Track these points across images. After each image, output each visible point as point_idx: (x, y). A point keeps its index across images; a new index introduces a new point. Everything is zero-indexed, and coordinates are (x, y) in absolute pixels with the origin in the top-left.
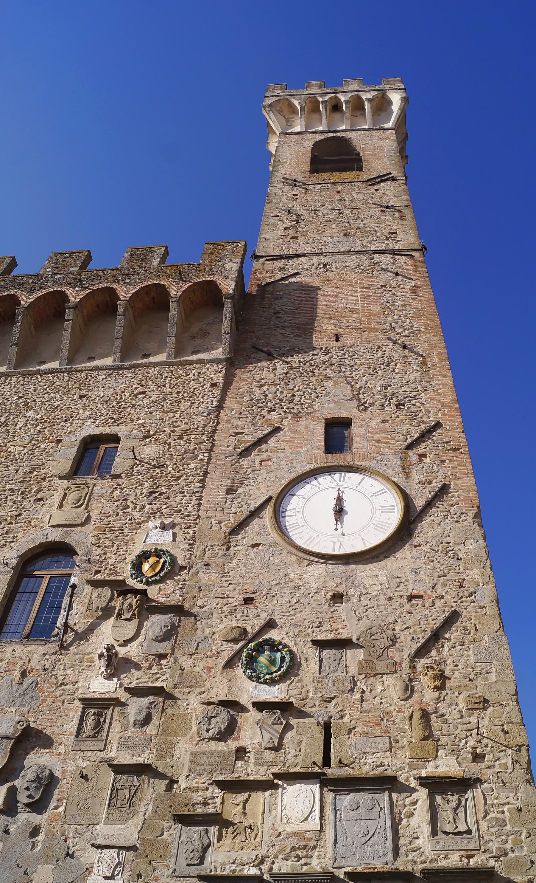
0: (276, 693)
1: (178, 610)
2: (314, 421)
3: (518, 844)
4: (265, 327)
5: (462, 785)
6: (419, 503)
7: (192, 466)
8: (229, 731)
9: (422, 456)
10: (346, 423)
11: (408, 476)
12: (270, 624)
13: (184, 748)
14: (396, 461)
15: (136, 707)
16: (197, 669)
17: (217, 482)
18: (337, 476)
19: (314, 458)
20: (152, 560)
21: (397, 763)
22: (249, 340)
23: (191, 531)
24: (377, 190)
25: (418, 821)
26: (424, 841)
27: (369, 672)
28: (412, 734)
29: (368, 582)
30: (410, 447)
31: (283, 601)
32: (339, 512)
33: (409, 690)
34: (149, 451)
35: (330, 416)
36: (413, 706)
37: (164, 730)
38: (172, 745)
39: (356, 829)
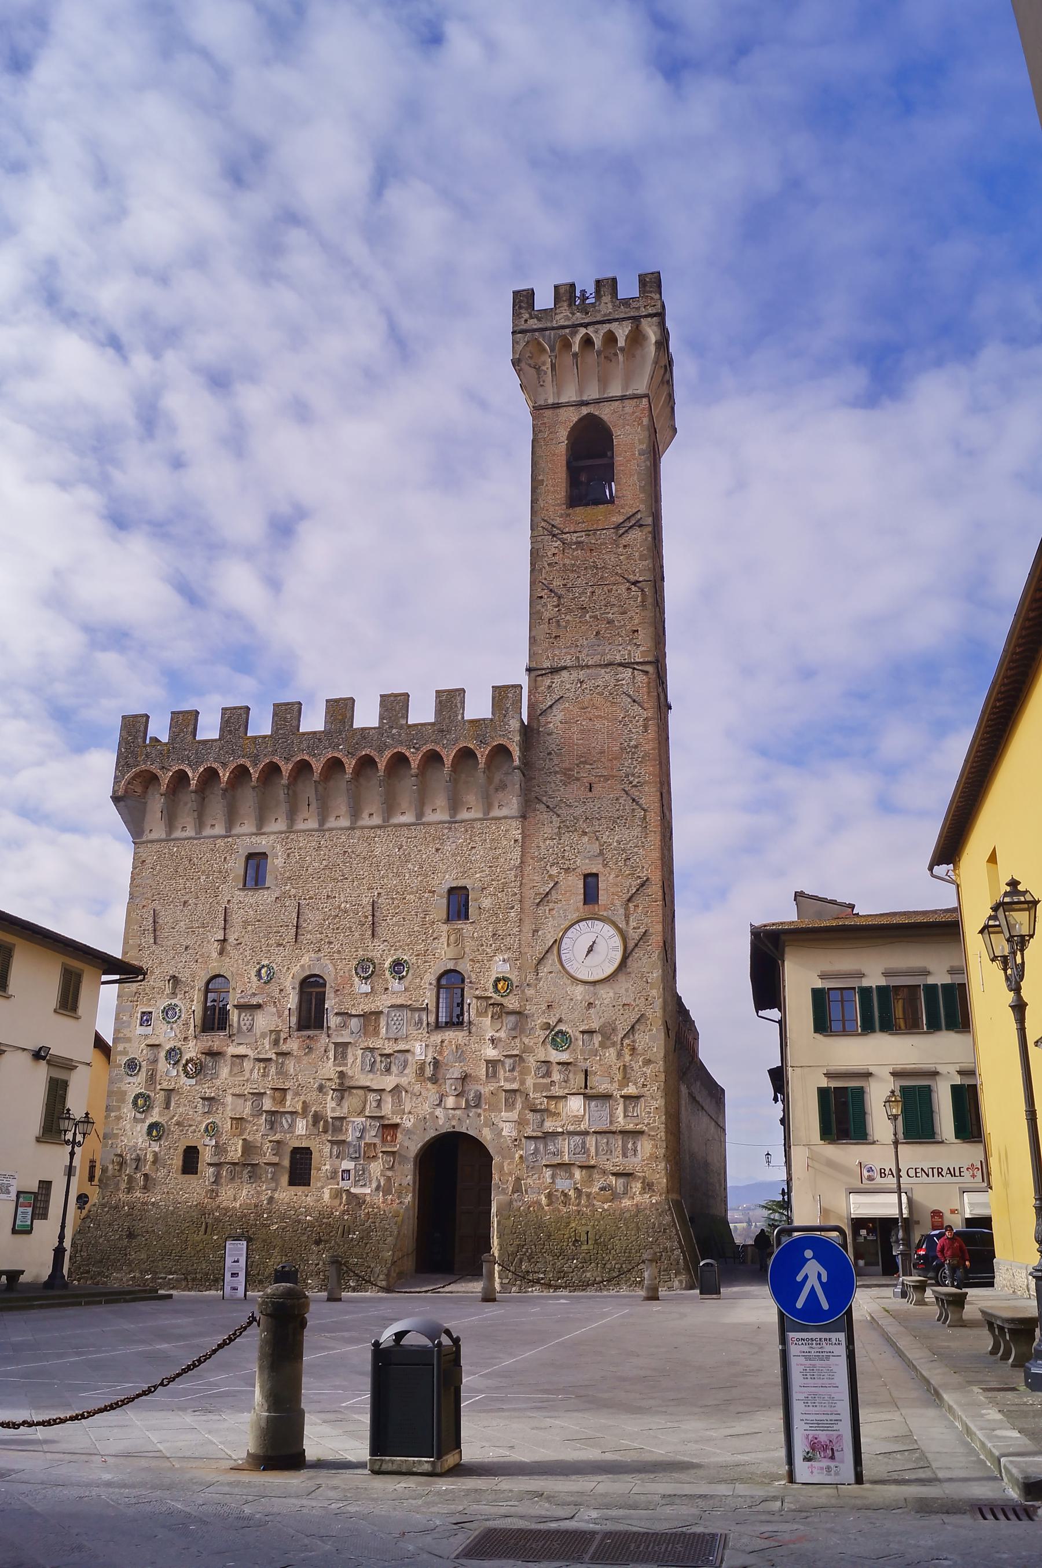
0: (564, 1057)
1: (519, 1013)
3: (654, 1121)
5: (637, 1098)
6: (631, 944)
8: (548, 1074)
9: (637, 906)
10: (596, 875)
11: (627, 923)
12: (560, 1021)
13: (530, 1082)
14: (622, 911)
15: (509, 1062)
17: (528, 928)
18: (590, 922)
19: (578, 909)
20: (502, 983)
21: (612, 1088)
23: (518, 962)
24: (625, 546)
25: (620, 1111)
26: (621, 1119)
27: (602, 1045)
28: (619, 1076)
29: (604, 996)
30: (629, 900)
31: (565, 1007)
32: (590, 950)
33: (619, 1055)
35: (586, 872)
36: (620, 1064)
37: (521, 1073)
39: (596, 1114)
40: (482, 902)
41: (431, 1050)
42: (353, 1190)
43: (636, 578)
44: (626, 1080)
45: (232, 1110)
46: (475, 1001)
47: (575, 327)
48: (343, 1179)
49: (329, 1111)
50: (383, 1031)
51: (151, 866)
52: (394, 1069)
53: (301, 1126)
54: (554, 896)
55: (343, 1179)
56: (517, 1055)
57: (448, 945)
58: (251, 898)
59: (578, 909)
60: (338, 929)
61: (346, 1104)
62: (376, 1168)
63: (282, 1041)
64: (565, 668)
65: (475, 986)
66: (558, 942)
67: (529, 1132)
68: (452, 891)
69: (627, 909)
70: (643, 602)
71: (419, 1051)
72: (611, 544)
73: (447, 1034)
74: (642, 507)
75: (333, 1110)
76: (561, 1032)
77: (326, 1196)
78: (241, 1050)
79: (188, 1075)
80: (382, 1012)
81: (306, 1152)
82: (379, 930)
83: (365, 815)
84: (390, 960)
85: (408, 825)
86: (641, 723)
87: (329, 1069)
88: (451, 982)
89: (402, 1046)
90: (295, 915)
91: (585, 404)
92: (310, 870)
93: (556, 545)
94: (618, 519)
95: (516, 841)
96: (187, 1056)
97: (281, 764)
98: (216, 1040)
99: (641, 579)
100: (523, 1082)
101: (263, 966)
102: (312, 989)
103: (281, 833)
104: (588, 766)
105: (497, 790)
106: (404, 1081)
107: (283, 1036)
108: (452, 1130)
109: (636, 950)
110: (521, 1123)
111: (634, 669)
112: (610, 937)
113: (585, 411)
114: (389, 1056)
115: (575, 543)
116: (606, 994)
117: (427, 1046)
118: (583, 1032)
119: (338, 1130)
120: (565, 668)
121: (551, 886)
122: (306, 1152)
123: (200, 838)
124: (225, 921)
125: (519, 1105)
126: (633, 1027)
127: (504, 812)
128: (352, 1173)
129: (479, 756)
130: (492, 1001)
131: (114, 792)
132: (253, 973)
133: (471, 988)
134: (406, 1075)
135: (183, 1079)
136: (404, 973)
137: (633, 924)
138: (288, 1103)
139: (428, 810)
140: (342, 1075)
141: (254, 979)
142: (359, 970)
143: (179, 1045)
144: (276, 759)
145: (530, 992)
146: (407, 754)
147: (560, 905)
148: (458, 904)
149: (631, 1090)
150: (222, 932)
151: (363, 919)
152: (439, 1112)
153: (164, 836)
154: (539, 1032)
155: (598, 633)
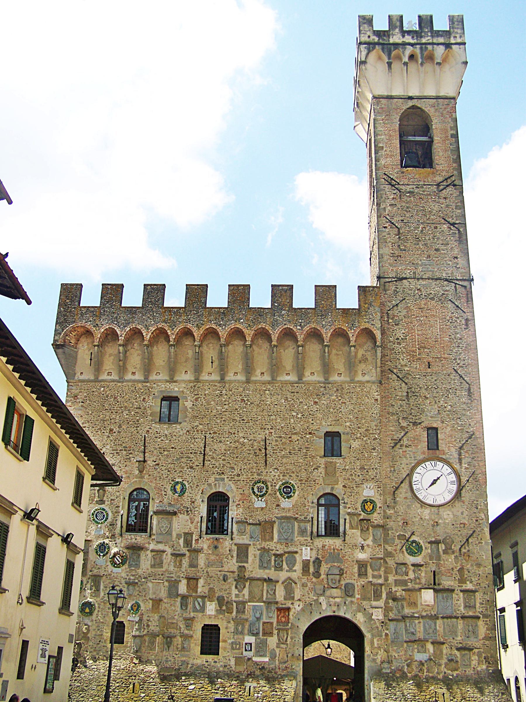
2: (422, 428)
4: (393, 352)
7: (374, 454)
14: (456, 456)
16: (391, 550)
19: (424, 453)
22: (387, 363)
24: (445, 198)
26: (462, 608)
32: (434, 482)
34: (355, 444)
37: (385, 572)
38: (388, 577)
40: (351, 445)
41: (314, 552)
42: (254, 659)
43: (453, 221)
44: (462, 581)
45: (154, 593)
46: (347, 517)
47: (404, 44)
48: (246, 650)
49: (233, 596)
50: (276, 536)
51: (81, 400)
52: (285, 566)
53: (211, 608)
54: (405, 442)
55: (246, 650)
56: (381, 559)
57: (326, 473)
58: (165, 430)
59: (424, 453)
60: (237, 457)
61: (246, 591)
62: (272, 641)
63: (194, 542)
64: (406, 278)
65: (348, 506)
66: (410, 475)
67: (391, 615)
68: (327, 434)
69: (460, 454)
70: (460, 238)
71: (307, 554)
72: (434, 195)
73: (327, 541)
74: (455, 173)
75: (237, 596)
76: (414, 542)
77: (233, 662)
78: (161, 547)
79: (114, 564)
80: (275, 522)
81: (216, 628)
82: (269, 460)
83: (258, 372)
84: (280, 483)
85: (292, 383)
86: (463, 322)
87: (232, 564)
88: (331, 502)
89: (291, 549)
90: (202, 445)
91: (411, 98)
92: (215, 411)
93: (395, 192)
94: (439, 179)
95: (377, 400)
96: (114, 550)
97: (194, 330)
98: (139, 538)
99: (457, 222)
100: (386, 579)
101: (178, 483)
102: (218, 502)
103: (190, 381)
104: (426, 350)
105: (360, 362)
106: (294, 575)
107: (194, 537)
108: (332, 614)
109: (468, 484)
110: (387, 610)
111: (456, 284)
112: (449, 474)
113: (410, 103)
114: (281, 555)
115: (409, 192)
116: (447, 515)
117: (311, 549)
118: (431, 543)
119: (241, 610)
120: (406, 278)
121: (402, 434)
122: (216, 628)
123: (123, 382)
124: (145, 447)
125: (384, 596)
126: (467, 540)
127: (367, 378)
128: (253, 645)
129: (351, 335)
130: (362, 517)
131: (55, 341)
132: (169, 487)
133: (345, 507)
134: (295, 571)
135: (110, 568)
136: (292, 494)
137: (464, 465)
138: (199, 590)
139: (307, 373)
140: (242, 569)
141: (170, 493)
142: (256, 490)
143: (107, 541)
144: (189, 326)
145: (390, 512)
146: (295, 330)
147: (410, 449)
148: (333, 443)
149: (469, 586)
150: (142, 455)
151: (257, 451)
152: (322, 599)
153: (92, 378)
154: (397, 541)
155: (429, 256)
